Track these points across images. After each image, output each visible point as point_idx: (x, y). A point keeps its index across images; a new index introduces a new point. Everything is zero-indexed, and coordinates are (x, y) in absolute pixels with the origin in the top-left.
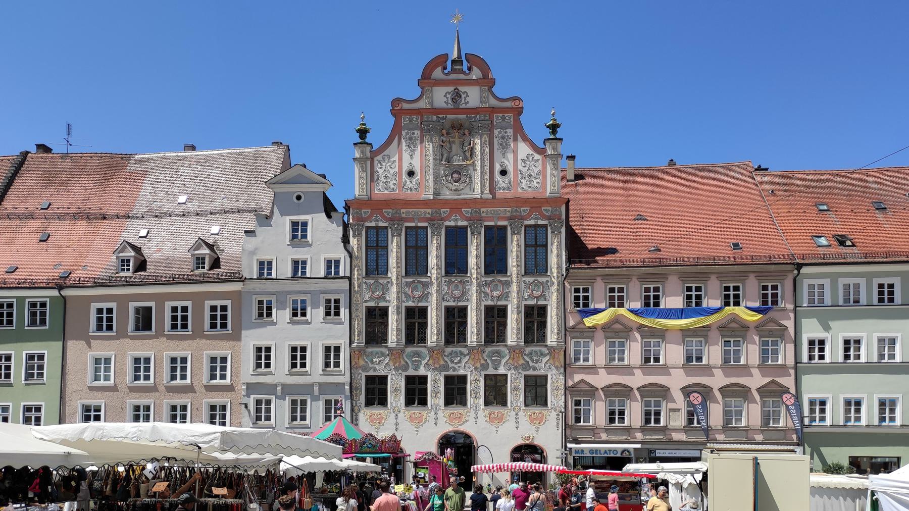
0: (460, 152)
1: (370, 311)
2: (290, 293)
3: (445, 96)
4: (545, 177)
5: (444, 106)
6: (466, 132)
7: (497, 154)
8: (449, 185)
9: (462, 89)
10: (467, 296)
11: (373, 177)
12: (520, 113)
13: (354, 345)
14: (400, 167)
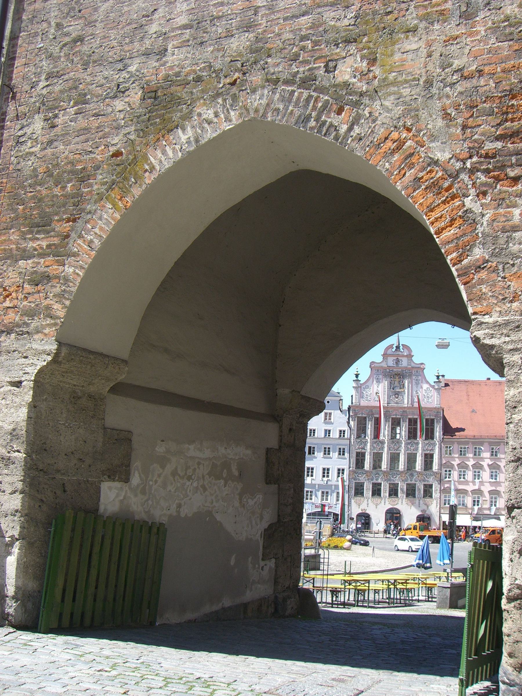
0: (398, 385)
1: (358, 454)
7: (414, 387)
10: (400, 449)
11: (361, 396)
13: (351, 469)
14: (373, 391)
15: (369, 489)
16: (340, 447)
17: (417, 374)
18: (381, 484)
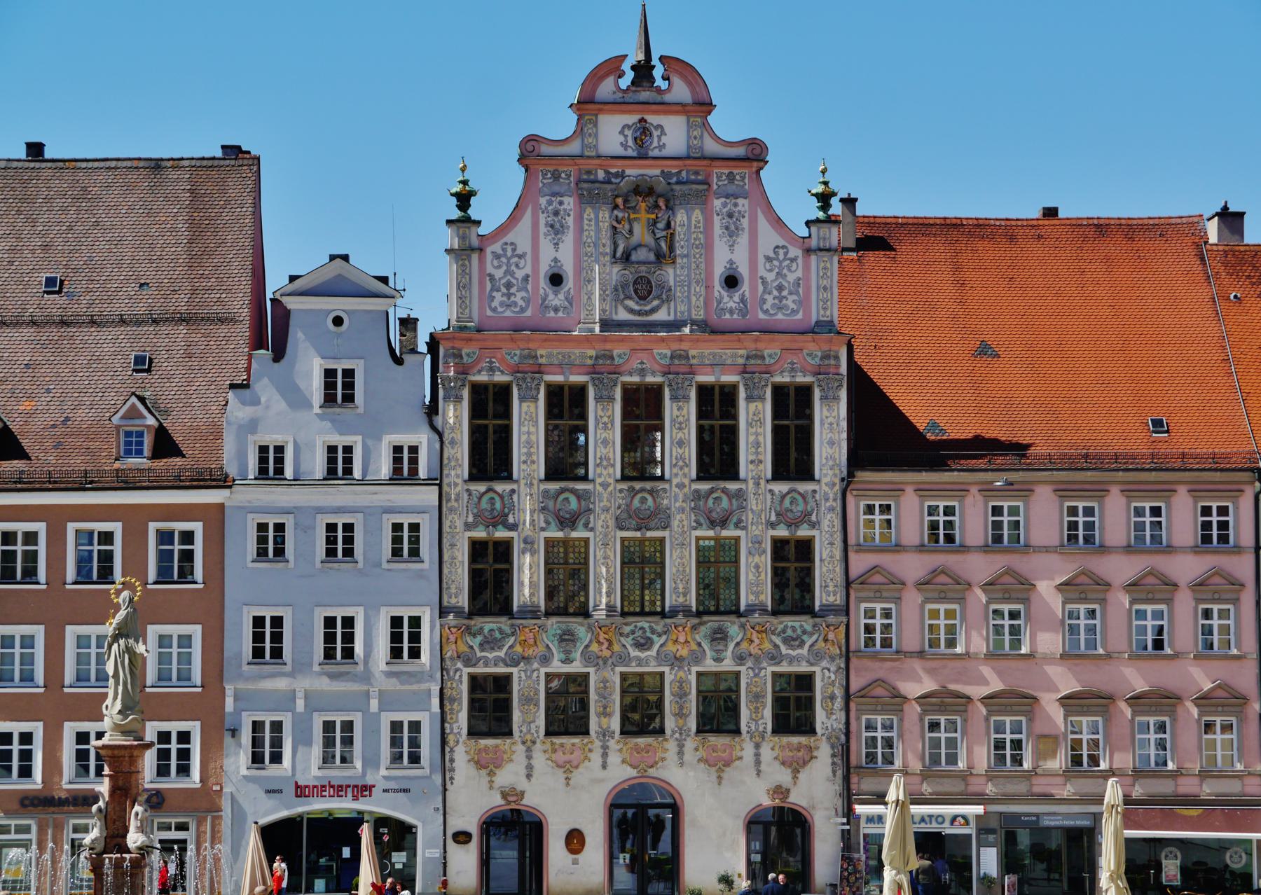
2: (321, 510)
3: (622, 132)
4: (808, 289)
5: (620, 151)
6: (661, 203)
8: (630, 303)
9: (653, 119)
15: (537, 705)
16: (398, 519)
17: (731, 189)
18: (586, 676)
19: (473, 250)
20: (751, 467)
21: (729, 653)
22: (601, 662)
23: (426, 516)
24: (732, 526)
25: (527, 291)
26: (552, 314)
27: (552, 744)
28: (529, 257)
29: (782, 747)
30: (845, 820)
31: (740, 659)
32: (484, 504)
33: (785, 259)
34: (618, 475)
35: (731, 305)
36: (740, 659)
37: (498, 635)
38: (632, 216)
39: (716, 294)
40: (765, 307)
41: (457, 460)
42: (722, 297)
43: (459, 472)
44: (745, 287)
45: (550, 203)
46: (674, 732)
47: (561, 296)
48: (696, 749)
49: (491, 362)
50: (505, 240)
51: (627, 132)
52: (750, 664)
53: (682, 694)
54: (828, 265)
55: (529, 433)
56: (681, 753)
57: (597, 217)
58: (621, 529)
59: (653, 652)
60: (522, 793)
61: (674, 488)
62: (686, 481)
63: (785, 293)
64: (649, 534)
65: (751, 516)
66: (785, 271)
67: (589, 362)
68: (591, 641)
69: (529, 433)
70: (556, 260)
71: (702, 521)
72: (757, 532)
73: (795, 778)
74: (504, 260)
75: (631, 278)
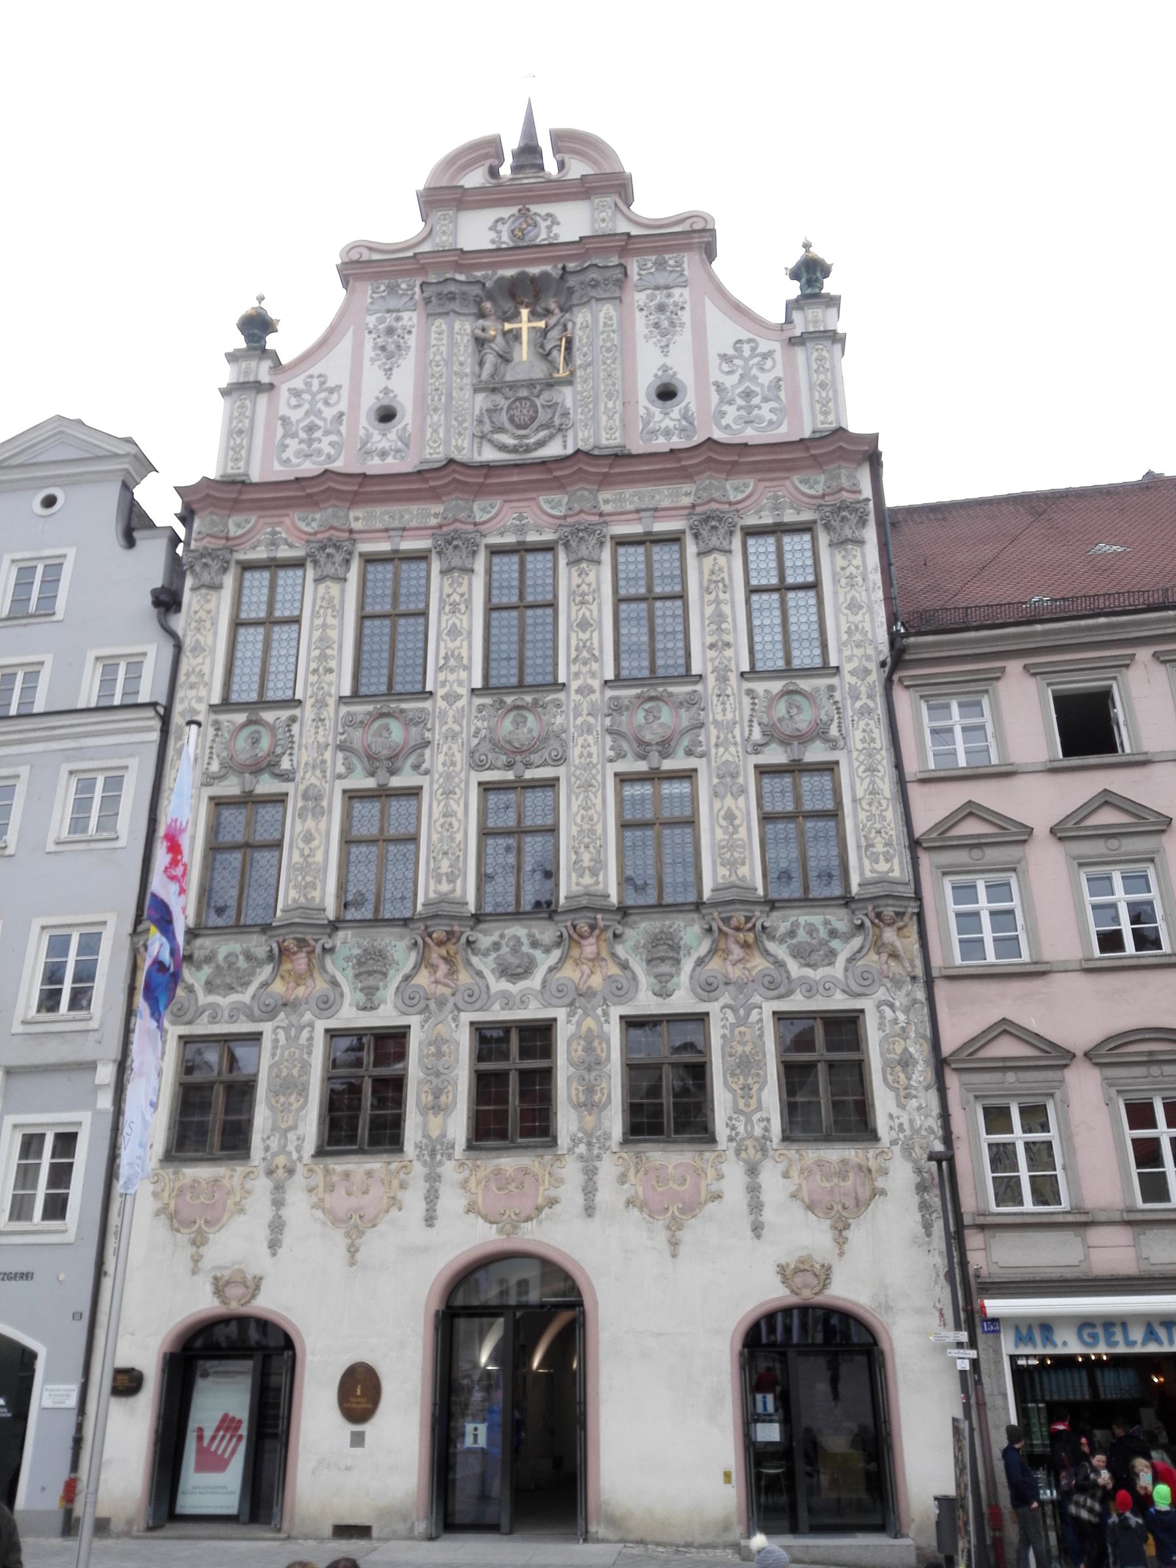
3: (493, 228)
12: (710, 252)
14: (354, 404)
15: (303, 1091)
17: (662, 278)
19: (258, 387)
20: (711, 654)
21: (684, 977)
22: (433, 1005)
23: (133, 763)
24: (681, 752)
25: (339, 433)
26: (377, 461)
27: (327, 1172)
28: (345, 392)
29: (806, 1172)
30: (964, 1336)
31: (708, 989)
32: (242, 742)
33: (753, 356)
34: (478, 683)
35: (668, 423)
36: (708, 989)
37: (242, 963)
38: (507, 326)
39: (642, 412)
40: (724, 422)
41: (201, 675)
42: (650, 415)
43: (203, 692)
44: (689, 398)
45: (381, 321)
46: (575, 1141)
47: (392, 435)
48: (623, 1179)
49: (274, 533)
50: (310, 372)
51: (500, 227)
52: (726, 999)
53: (592, 1064)
54: (825, 354)
55: (325, 626)
56: (589, 1191)
57: (451, 329)
58: (480, 766)
59: (535, 982)
60: (258, 1281)
61: (574, 696)
62: (596, 684)
63: (756, 401)
64: (529, 774)
65: (714, 732)
66: (754, 371)
67: (433, 522)
68: (416, 968)
69: (325, 626)
70: (386, 391)
71: (626, 746)
72: (727, 757)
73: (841, 1241)
74: (306, 396)
75: (504, 403)
